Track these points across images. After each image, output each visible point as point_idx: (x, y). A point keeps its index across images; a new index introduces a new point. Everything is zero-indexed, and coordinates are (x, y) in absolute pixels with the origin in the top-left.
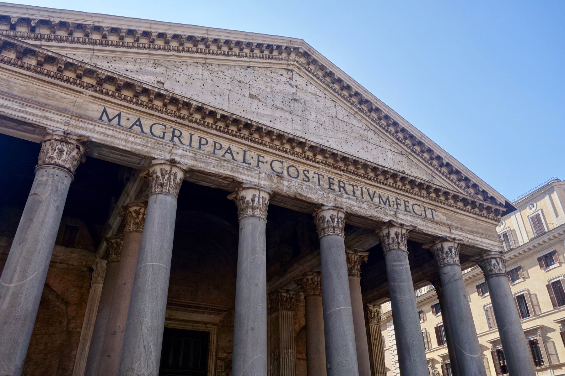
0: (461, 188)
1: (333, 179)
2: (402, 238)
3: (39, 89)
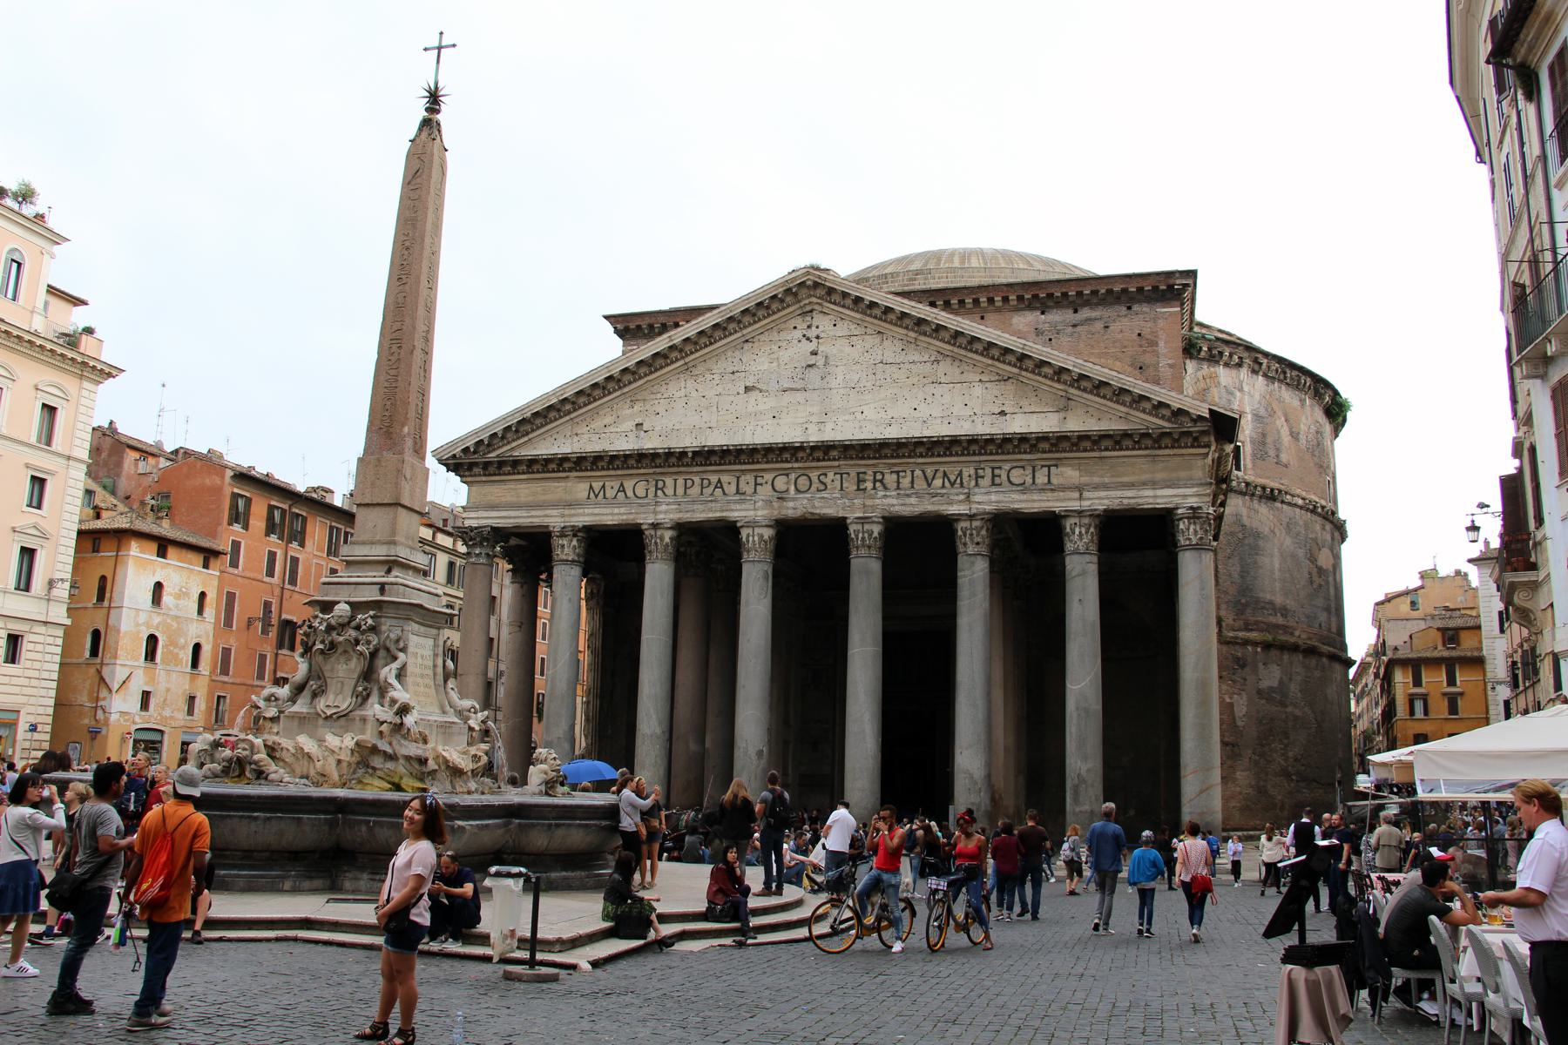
0: (1124, 404)
1: (865, 473)
2: (971, 535)
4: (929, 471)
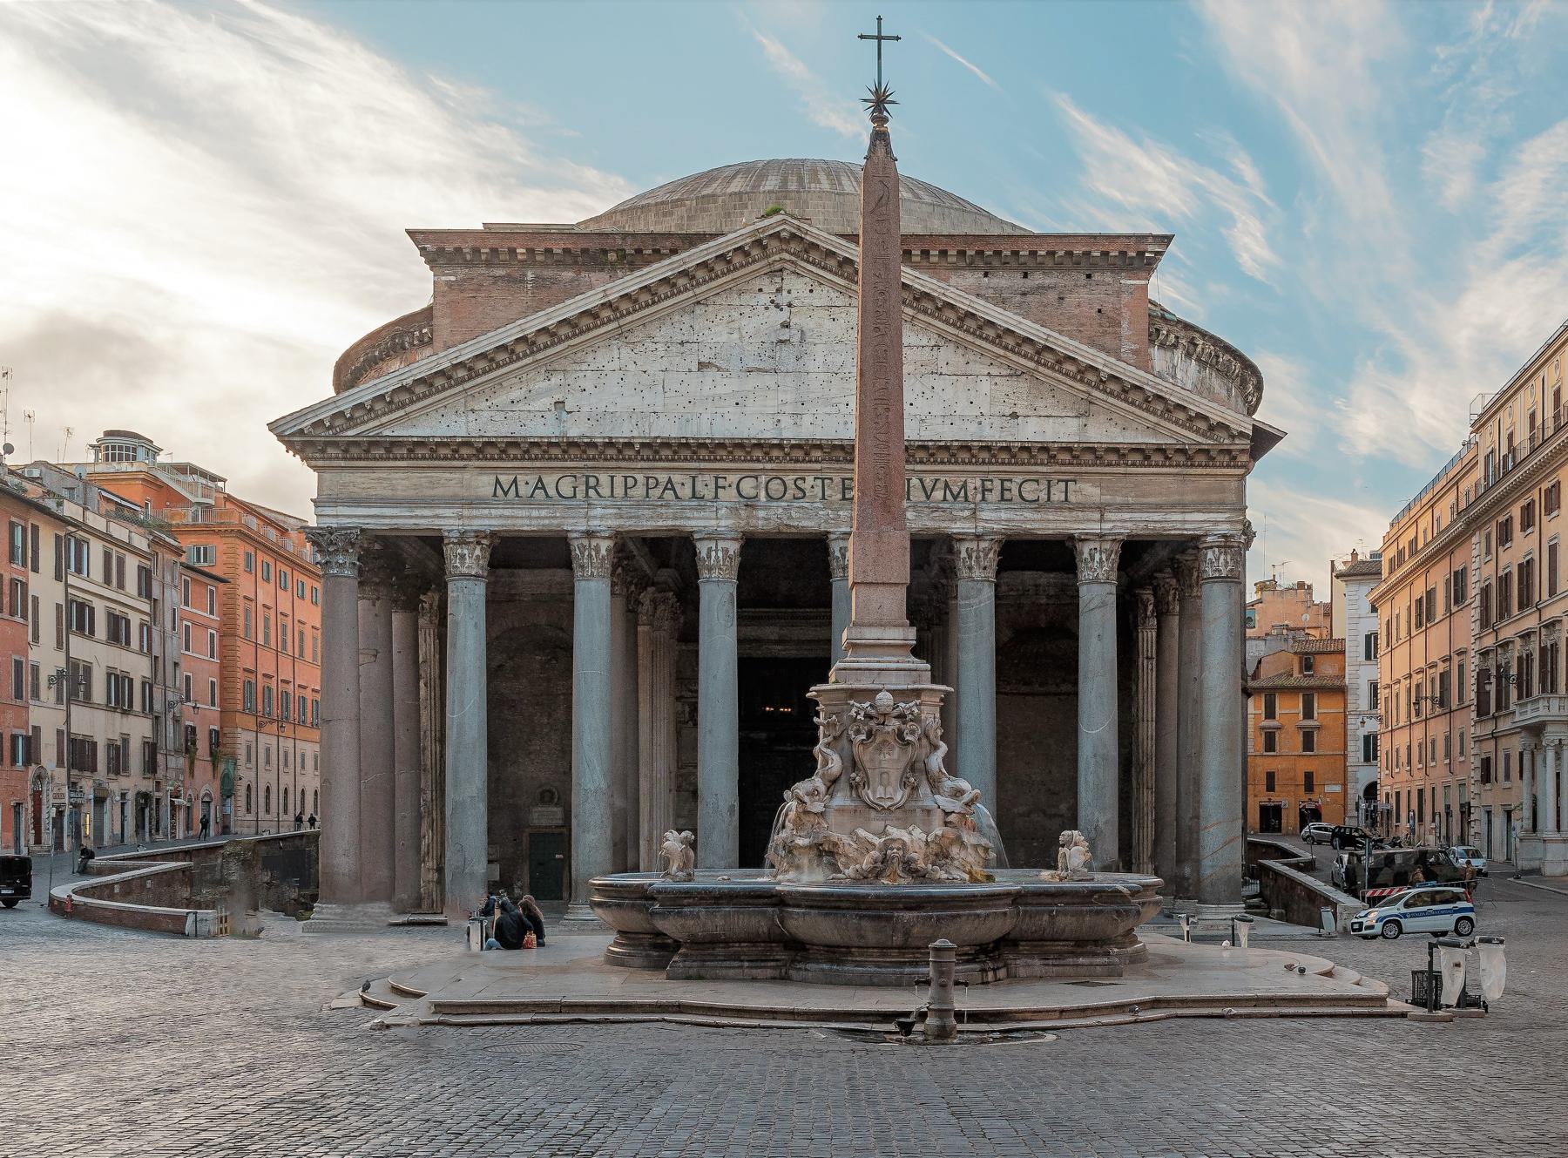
0: (1154, 413)
4: (928, 480)
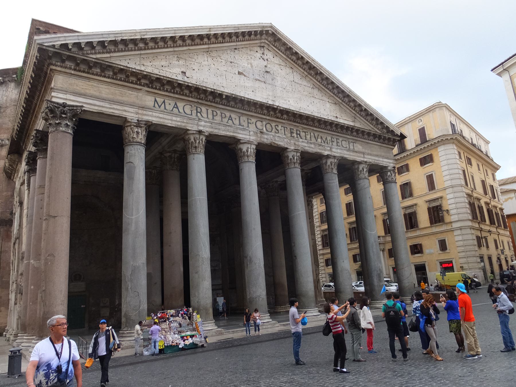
0: (372, 125)
1: (293, 129)
2: (334, 165)
3: (115, 90)
